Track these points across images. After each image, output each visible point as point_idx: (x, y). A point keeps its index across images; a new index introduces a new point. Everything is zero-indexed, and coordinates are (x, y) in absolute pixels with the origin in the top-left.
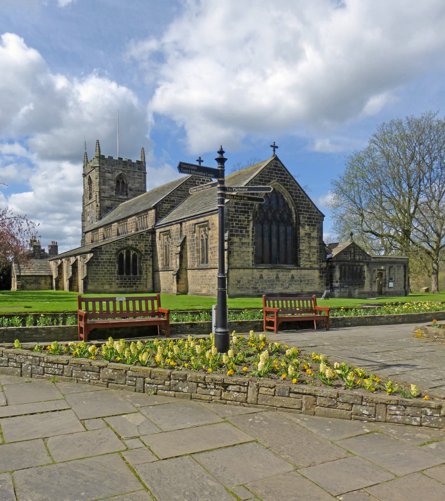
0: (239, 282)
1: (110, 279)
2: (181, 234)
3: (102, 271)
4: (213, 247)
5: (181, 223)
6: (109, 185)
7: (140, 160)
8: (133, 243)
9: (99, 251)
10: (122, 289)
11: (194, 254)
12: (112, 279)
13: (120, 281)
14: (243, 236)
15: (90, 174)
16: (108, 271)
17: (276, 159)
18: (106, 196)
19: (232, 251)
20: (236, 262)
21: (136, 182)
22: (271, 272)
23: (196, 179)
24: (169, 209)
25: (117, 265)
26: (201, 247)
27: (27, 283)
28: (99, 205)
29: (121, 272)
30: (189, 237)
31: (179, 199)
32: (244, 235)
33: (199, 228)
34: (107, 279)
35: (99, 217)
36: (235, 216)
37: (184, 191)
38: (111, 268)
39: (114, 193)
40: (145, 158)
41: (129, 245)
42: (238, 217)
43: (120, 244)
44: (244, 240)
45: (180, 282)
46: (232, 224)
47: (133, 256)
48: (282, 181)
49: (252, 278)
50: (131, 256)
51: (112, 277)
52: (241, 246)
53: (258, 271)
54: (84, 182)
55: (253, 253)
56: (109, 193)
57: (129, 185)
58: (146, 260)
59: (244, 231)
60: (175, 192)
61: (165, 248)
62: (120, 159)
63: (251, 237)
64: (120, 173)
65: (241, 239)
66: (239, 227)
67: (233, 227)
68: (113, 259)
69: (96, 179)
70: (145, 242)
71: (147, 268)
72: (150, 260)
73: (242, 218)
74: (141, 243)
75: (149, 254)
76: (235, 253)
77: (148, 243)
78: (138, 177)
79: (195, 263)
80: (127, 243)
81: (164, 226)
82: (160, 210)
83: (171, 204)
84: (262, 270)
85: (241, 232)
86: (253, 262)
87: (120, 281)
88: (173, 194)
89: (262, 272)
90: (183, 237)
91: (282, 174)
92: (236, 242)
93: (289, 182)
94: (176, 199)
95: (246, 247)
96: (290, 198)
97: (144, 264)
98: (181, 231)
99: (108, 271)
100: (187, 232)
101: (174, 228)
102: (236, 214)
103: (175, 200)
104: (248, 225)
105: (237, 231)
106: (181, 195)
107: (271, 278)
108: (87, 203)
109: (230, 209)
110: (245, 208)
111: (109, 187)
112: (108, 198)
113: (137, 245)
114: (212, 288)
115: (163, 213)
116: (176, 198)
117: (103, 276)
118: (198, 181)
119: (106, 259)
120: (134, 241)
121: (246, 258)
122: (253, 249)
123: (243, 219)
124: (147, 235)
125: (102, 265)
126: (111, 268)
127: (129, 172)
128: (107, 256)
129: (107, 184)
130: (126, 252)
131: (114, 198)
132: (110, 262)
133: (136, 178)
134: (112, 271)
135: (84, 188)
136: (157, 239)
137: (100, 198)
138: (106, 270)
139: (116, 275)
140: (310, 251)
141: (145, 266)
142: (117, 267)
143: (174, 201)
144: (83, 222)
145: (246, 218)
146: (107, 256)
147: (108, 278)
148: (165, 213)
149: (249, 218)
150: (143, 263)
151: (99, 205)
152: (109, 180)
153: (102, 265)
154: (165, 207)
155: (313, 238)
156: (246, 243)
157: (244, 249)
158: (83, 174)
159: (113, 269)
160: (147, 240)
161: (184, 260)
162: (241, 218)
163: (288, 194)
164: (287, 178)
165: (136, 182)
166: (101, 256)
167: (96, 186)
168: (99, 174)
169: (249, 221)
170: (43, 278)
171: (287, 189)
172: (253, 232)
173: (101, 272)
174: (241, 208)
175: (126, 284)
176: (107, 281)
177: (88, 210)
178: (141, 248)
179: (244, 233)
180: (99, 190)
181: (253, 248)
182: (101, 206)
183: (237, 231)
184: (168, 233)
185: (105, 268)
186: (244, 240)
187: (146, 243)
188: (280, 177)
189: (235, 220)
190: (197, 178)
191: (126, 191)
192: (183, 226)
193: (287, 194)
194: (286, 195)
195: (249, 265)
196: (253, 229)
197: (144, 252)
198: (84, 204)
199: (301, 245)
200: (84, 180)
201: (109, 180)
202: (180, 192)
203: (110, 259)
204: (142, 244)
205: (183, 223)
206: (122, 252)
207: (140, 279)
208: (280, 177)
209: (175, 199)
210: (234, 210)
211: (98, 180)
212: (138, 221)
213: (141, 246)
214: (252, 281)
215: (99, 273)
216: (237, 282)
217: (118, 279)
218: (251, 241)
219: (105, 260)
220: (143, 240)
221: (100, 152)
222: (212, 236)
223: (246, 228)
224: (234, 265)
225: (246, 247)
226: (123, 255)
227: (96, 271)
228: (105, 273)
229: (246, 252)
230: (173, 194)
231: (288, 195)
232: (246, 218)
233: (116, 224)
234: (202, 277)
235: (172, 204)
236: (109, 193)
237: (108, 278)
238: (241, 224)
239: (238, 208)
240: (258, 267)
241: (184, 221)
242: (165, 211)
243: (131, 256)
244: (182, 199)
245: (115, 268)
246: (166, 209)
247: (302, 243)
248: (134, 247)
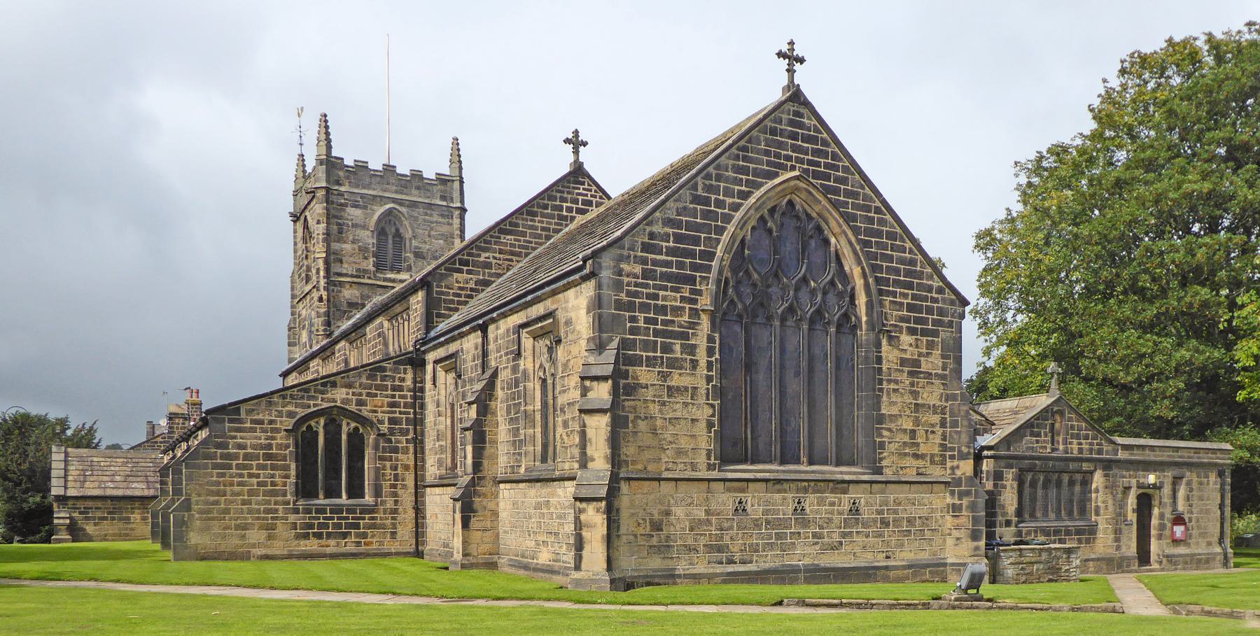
0: (657, 527)
1: (267, 511)
2: (484, 366)
3: (240, 484)
4: (568, 404)
5: (484, 329)
6: (352, 242)
8: (350, 396)
9: (231, 421)
10: (312, 545)
11: (518, 428)
12: (276, 511)
13: (304, 518)
14: (674, 364)
15: (307, 213)
16: (259, 484)
17: (795, 96)
19: (631, 417)
20: (647, 455)
21: (433, 233)
22: (779, 491)
23: (563, 200)
24: (472, 290)
25: (293, 466)
26: (538, 405)
28: (325, 297)
29: (306, 489)
30: (506, 371)
31: (507, 260)
32: (676, 359)
33: (534, 338)
34: (258, 511)
36: (645, 291)
37: (524, 234)
38: (273, 476)
39: (370, 264)
40: (461, 168)
41: (334, 401)
42: (656, 297)
43: (302, 397)
44: (677, 380)
45: (474, 523)
46: (633, 319)
47: (349, 435)
48: (817, 175)
49: (708, 512)
50: (344, 437)
51: (276, 503)
52: (666, 399)
53: (729, 490)
54: (295, 237)
55: (710, 425)
56: (355, 263)
58: (396, 450)
59: (678, 348)
60: (491, 236)
61: (449, 411)
62: (389, 169)
63: (702, 370)
64: (388, 206)
65: (664, 376)
66: (657, 333)
67: (634, 331)
68: (280, 446)
70: (389, 392)
71: (396, 477)
72: (406, 451)
73: (671, 298)
74: (376, 395)
75: (404, 432)
76: (642, 425)
77: (400, 397)
78: (440, 220)
79: (520, 461)
80: (329, 395)
81: (442, 339)
82: (443, 293)
83: (478, 274)
84: (745, 484)
85: (667, 349)
86: (709, 458)
87: (304, 518)
88: (486, 242)
89: (742, 491)
90: (487, 375)
91: (816, 153)
92: (646, 387)
93: (844, 181)
94: (495, 258)
95: (686, 404)
96: (846, 236)
97: (388, 464)
98: (485, 354)
99: (259, 484)
100: (501, 357)
101: (471, 343)
102: (646, 286)
103: (494, 261)
104: (693, 325)
105: (647, 346)
106: (512, 245)
107: (776, 512)
108: (302, 292)
109: (624, 266)
110: (681, 265)
111: (356, 246)
112: (352, 276)
113: (360, 403)
114: (565, 547)
115: (452, 302)
116: (497, 255)
117: (244, 503)
118: (569, 205)
119: (254, 447)
120: (351, 391)
121: (684, 443)
122: (711, 411)
123: (674, 303)
124: (396, 370)
125: (238, 467)
126: (273, 476)
127: (413, 205)
128: (256, 438)
129: (351, 238)
130: (325, 426)
131: (369, 278)
132: (268, 457)
133: (437, 222)
134: (273, 484)
135: (295, 251)
136: (428, 385)
137: (327, 276)
138: (255, 480)
139: (289, 497)
140: (917, 422)
141: (388, 471)
142: (293, 472)
143: (487, 265)
144: (291, 348)
145: (683, 299)
146: (256, 438)
147: (262, 508)
148: (459, 303)
149: (695, 301)
150: (381, 458)
151: (325, 297)
152: (355, 226)
153: (238, 467)
154: (457, 282)
155: (929, 375)
156: (686, 389)
157: (677, 408)
158: (292, 215)
159: (277, 479)
160: (400, 389)
161: (487, 452)
162: (665, 298)
163: (841, 221)
164: (836, 168)
165: (433, 233)
166: (235, 437)
168: (327, 209)
169: (695, 313)
170: (137, 504)
171: (835, 205)
172: (710, 352)
173: (236, 488)
174: (668, 264)
175: (321, 526)
176: (258, 518)
177: (304, 313)
178: (375, 412)
179: (679, 355)
180: (324, 255)
181: (712, 406)
182: (332, 299)
183: (647, 346)
184: (451, 363)
185: (250, 476)
186: (677, 380)
187: (393, 396)
188: (810, 163)
189: (645, 308)
190: (565, 195)
192: (491, 336)
193: (836, 220)
194: (833, 224)
195: (694, 467)
196: (710, 339)
197: (386, 425)
198: (293, 297)
199: (885, 398)
200: (295, 232)
201: (355, 226)
202: (509, 237)
203: (270, 446)
204: (382, 400)
205: (491, 328)
206: (313, 423)
207: (372, 511)
208: (810, 163)
209: (491, 260)
210: (638, 269)
211: (323, 225)
212: (391, 332)
213: (377, 407)
214: (709, 522)
215: (229, 493)
216: (648, 527)
217: (296, 511)
218: (702, 385)
219: (250, 451)
220: (385, 388)
221: (329, 147)
222: (565, 365)
223: (684, 336)
224: (640, 467)
225: (686, 404)
226: (317, 433)
227: (218, 484)
228: (251, 493)
229: (683, 422)
230: (486, 242)
231: (840, 226)
232: (683, 299)
233: (342, 343)
234: (538, 506)
235: (484, 275)
236: (355, 263)
237: (262, 508)
238: (665, 323)
239: (655, 263)
240: (730, 475)
241: (494, 321)
242: (459, 295)
243: (344, 437)
244: (514, 258)
245: (287, 477)
246: (461, 288)
247: (888, 394)
248: (353, 408)
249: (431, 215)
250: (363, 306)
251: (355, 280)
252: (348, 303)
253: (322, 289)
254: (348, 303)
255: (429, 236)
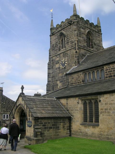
6: (83, 38)
7: (97, 24)
18: (81, 45)
27: (45, 128)
35: (77, 62)
54: (51, 40)
56: (83, 43)
57: (94, 41)
69: (75, 31)
129: (82, 37)
131: (86, 48)
135: (51, 43)
152: (83, 33)
167: (75, 36)
191: (92, 45)
236: (83, 43)
249: (96, 34)
250: (85, 56)
251: (83, 48)
252: (82, 54)
253: (77, 49)
254: (82, 54)
255: (96, 40)
